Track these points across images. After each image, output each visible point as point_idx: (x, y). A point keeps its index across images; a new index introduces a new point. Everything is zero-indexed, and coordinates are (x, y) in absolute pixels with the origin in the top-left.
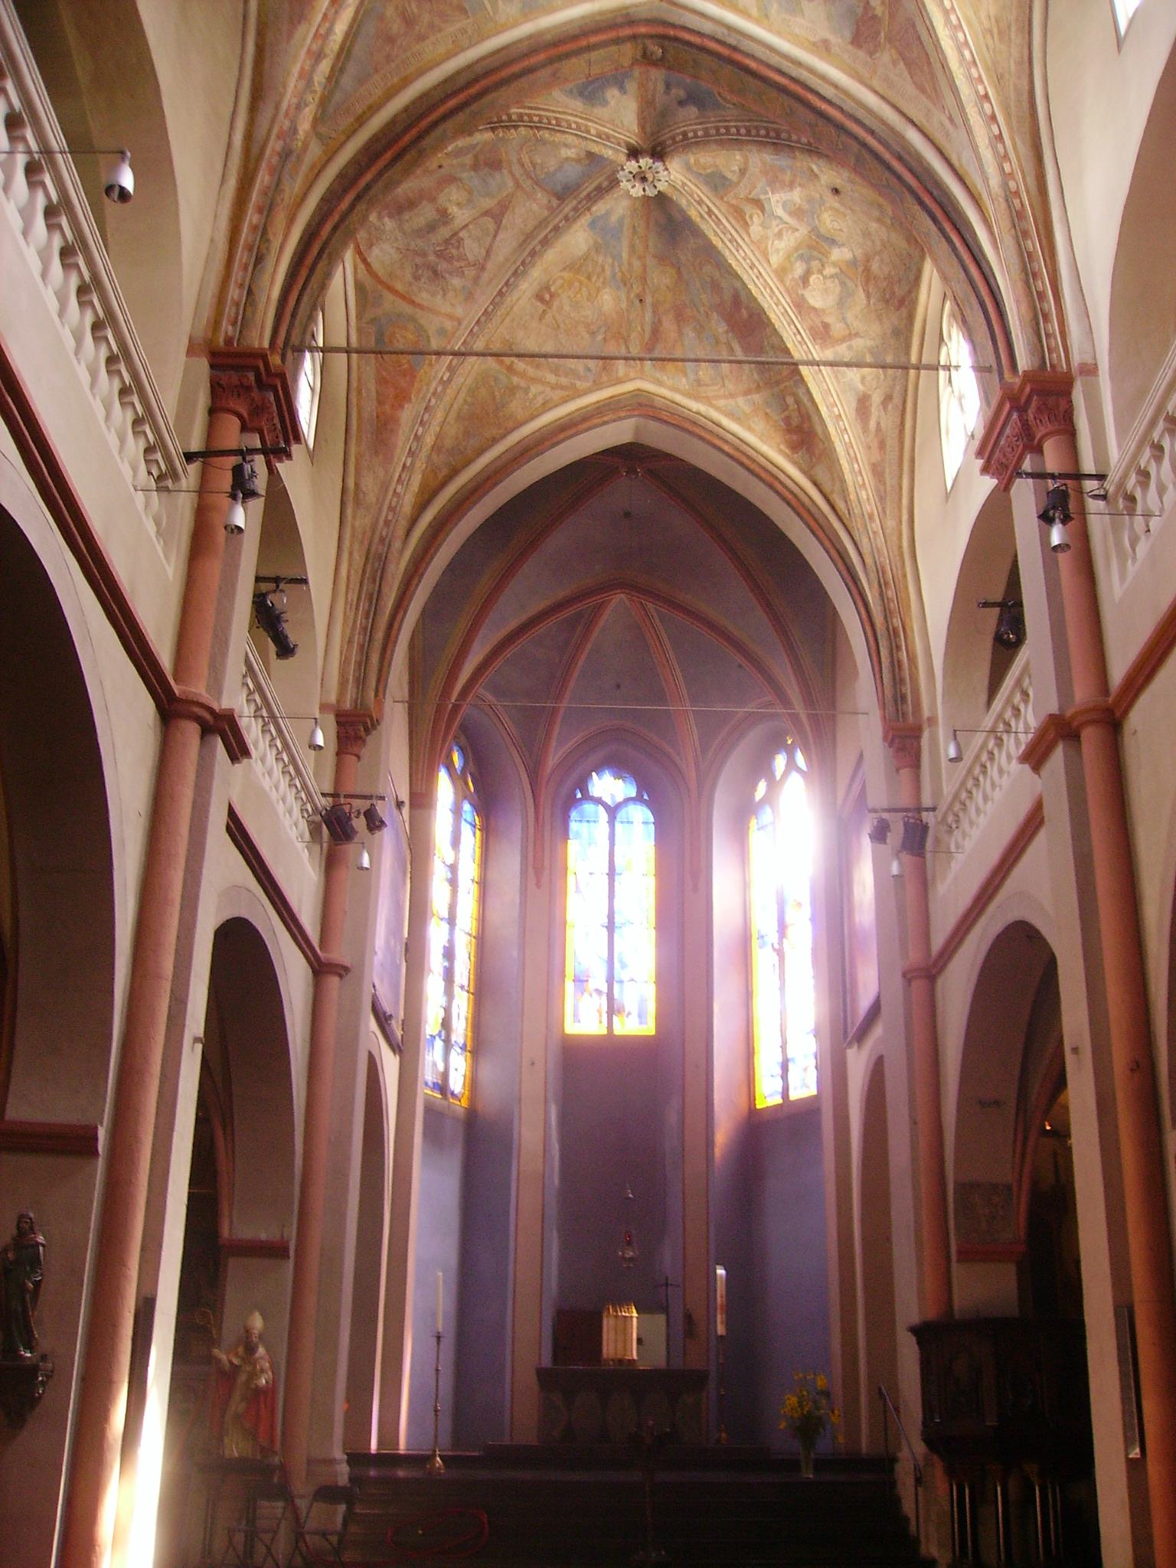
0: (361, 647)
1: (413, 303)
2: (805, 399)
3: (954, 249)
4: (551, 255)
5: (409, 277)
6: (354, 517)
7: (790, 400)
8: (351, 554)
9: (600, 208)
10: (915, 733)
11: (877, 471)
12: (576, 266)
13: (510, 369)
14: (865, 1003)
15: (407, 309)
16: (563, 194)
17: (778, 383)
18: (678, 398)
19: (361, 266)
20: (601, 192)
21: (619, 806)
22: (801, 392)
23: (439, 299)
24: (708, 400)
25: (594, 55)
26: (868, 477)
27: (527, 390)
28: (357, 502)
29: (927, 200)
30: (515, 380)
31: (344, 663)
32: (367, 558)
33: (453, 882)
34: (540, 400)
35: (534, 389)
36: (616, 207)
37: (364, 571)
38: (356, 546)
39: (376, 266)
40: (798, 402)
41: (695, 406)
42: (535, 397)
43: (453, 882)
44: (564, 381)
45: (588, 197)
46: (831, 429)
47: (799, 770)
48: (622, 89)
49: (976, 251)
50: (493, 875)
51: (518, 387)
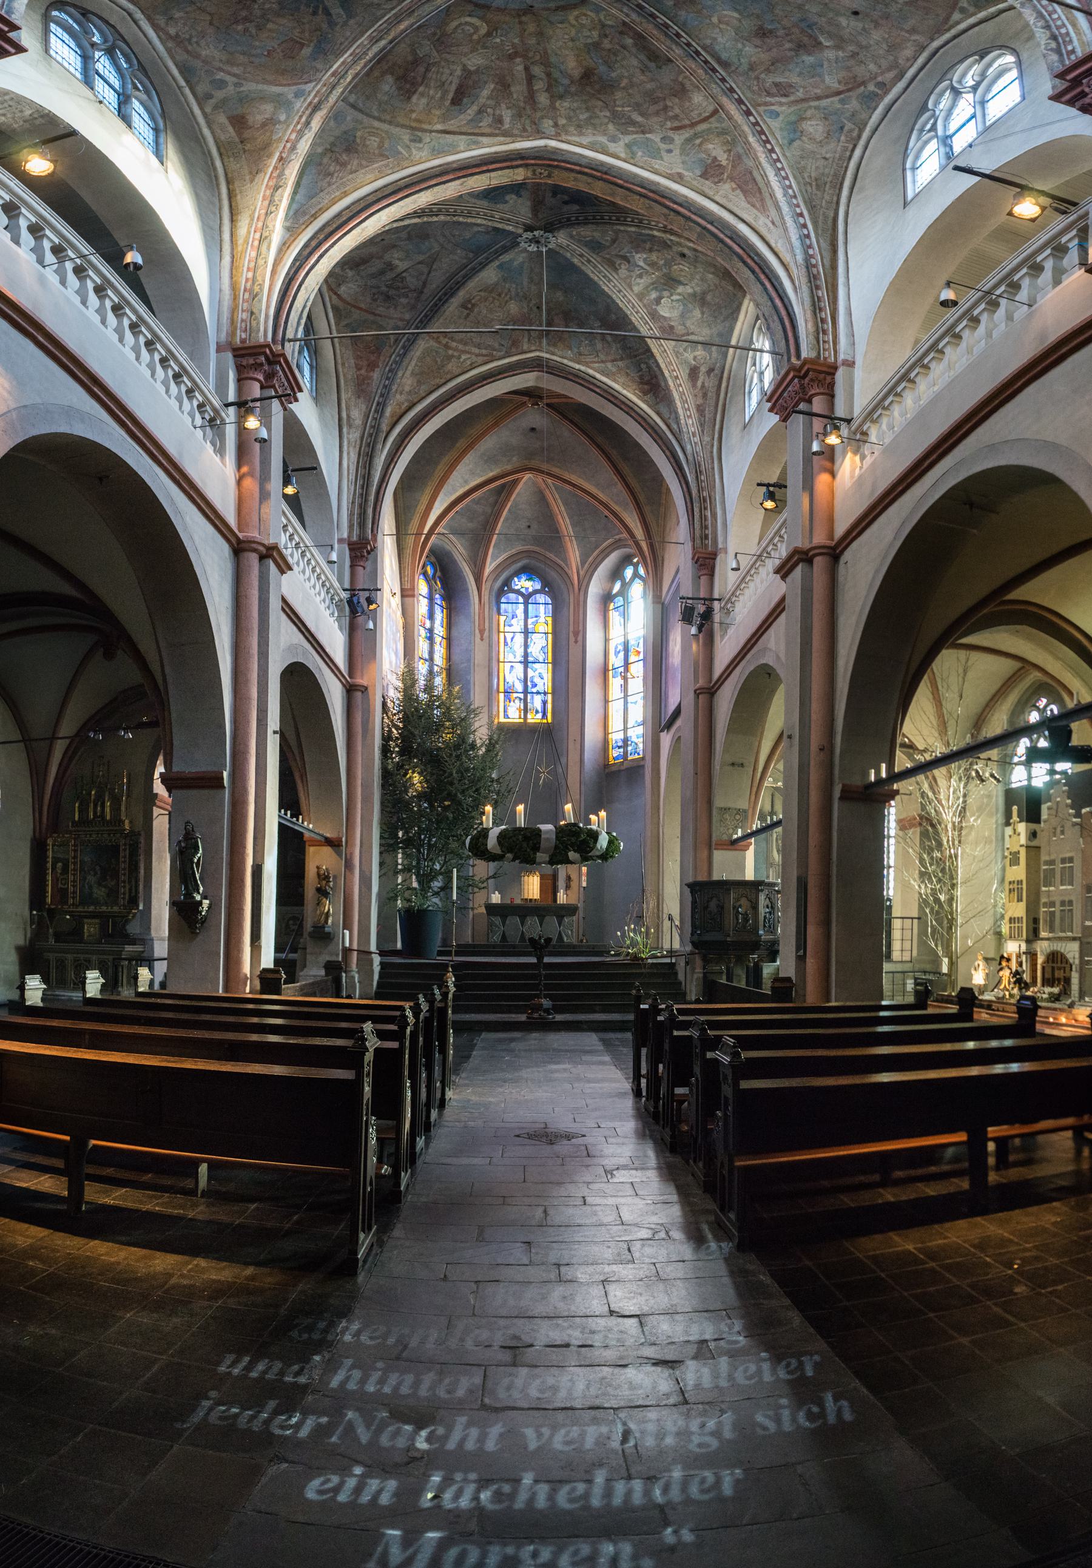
0: (360, 506)
1: (376, 315)
2: (654, 366)
3: (766, 289)
4: (471, 284)
5: (369, 300)
6: (348, 433)
7: (643, 366)
8: (348, 453)
9: (506, 258)
10: (713, 556)
11: (700, 410)
12: (489, 289)
13: (447, 347)
14: (672, 707)
15: (371, 317)
16: (478, 251)
17: (636, 356)
18: (565, 361)
19: (334, 297)
20: (505, 249)
21: (531, 595)
22: (651, 361)
23: (392, 311)
24: (587, 364)
25: (493, 174)
26: (693, 411)
27: (459, 357)
28: (350, 426)
29: (749, 261)
30: (450, 352)
31: (351, 515)
32: (359, 454)
33: (431, 638)
34: (469, 362)
35: (463, 357)
36: (516, 258)
37: (358, 462)
38: (351, 449)
39: (345, 296)
40: (649, 367)
41: (577, 366)
42: (465, 360)
43: (431, 638)
44: (484, 352)
45: (496, 252)
46: (671, 383)
47: (641, 577)
48: (519, 196)
49: (781, 291)
50: (454, 633)
51: (453, 356)
